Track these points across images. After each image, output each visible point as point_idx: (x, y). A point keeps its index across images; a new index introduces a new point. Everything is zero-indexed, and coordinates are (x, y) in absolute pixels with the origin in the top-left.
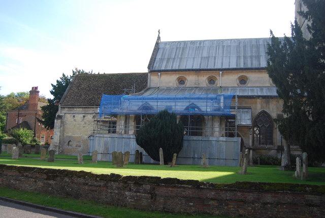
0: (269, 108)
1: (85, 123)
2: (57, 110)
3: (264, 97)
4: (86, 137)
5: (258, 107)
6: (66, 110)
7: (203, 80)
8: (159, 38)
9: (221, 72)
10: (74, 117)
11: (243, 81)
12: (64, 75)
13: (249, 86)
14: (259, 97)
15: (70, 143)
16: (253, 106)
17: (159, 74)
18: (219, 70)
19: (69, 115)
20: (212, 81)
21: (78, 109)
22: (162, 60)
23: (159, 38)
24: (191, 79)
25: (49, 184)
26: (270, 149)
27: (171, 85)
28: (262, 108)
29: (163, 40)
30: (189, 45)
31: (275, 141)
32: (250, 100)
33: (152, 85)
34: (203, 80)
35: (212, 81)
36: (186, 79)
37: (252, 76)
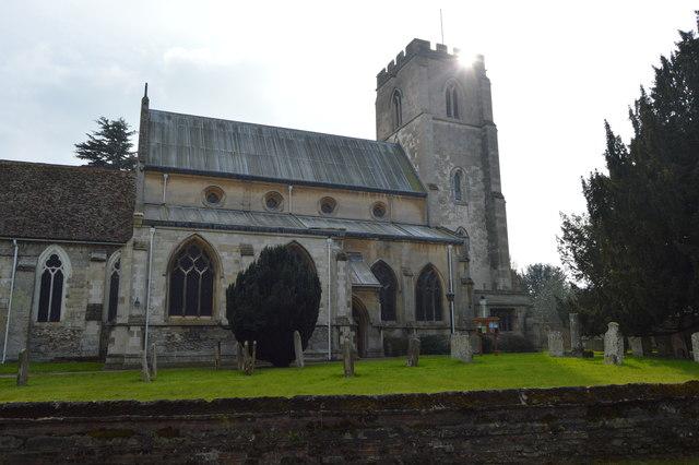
0: (389, 257)
3: (382, 238)
5: (373, 252)
7: (258, 196)
8: (145, 101)
11: (328, 206)
13: (338, 215)
14: (374, 236)
17: (166, 175)
20: (273, 201)
22: (165, 147)
23: (145, 101)
24: (233, 194)
25: (612, 429)
26: (392, 328)
27: (191, 201)
29: (151, 106)
30: (215, 127)
31: (399, 313)
33: (148, 199)
34: (258, 196)
35: (273, 201)
36: (222, 192)
37: (343, 200)
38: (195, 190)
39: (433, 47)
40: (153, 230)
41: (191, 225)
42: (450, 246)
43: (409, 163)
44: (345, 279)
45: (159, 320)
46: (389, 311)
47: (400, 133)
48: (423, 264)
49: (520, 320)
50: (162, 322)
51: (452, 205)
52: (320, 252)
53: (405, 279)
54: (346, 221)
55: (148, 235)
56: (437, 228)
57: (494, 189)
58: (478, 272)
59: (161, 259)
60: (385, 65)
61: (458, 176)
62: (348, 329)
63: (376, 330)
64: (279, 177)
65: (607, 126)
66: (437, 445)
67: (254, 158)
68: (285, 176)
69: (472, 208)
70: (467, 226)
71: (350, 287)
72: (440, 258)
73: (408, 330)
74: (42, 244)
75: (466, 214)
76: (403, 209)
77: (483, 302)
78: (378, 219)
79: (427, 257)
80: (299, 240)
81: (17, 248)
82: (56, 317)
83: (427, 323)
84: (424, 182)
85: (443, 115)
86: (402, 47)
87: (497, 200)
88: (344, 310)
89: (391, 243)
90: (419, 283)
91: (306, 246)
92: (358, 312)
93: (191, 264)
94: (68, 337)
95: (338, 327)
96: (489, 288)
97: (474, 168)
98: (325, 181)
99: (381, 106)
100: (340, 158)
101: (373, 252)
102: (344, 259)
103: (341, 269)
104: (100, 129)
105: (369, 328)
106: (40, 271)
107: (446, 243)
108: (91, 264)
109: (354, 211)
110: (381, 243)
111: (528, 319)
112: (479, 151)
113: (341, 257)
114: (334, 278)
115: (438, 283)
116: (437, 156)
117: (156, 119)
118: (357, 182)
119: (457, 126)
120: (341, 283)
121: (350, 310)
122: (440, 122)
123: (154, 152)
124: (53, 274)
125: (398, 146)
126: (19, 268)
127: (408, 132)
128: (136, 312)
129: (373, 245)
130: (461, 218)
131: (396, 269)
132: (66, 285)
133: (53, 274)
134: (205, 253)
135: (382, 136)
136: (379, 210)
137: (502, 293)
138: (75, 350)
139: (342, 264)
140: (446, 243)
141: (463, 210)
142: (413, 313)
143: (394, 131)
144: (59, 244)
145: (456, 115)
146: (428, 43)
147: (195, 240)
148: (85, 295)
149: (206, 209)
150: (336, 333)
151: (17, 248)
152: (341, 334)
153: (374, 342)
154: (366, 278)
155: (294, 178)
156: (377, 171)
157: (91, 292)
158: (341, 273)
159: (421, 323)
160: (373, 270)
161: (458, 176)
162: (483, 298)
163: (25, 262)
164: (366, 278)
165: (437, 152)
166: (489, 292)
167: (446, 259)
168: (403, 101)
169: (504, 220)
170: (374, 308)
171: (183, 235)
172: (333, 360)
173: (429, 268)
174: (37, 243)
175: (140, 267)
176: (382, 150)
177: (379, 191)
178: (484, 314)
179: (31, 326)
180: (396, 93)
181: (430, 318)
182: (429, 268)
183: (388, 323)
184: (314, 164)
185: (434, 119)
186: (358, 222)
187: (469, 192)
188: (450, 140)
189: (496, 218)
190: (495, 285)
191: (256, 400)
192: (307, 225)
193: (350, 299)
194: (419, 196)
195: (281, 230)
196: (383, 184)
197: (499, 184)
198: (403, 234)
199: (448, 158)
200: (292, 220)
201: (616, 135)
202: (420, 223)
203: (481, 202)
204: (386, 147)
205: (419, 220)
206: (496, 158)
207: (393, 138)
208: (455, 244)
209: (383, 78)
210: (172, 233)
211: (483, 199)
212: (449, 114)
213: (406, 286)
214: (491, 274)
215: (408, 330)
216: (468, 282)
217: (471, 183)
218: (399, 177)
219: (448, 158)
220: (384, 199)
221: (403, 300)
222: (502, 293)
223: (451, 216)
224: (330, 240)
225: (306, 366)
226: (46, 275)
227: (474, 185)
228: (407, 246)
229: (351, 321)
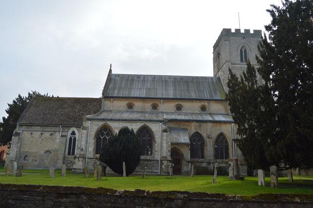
0: (201, 130)
1: (43, 140)
2: (15, 127)
3: (197, 121)
4: (43, 152)
5: (193, 128)
6: (24, 128)
7: (148, 106)
8: (110, 71)
10: (32, 134)
11: (179, 108)
12: (19, 96)
13: (183, 112)
14: (193, 121)
15: (26, 158)
16: (189, 128)
18: (161, 99)
19: (26, 133)
20: (155, 107)
21: (36, 127)
22: (114, 88)
23: (110, 71)
24: (138, 105)
26: (202, 162)
27: (121, 109)
29: (113, 72)
30: (136, 78)
31: (205, 155)
32: (186, 123)
33: (106, 109)
34: (148, 106)
35: (155, 107)
36: (134, 105)
37: (186, 105)
38: (123, 104)
40: (90, 122)
41: (103, 120)
42: (233, 124)
44: (166, 140)
45: (91, 156)
48: (218, 133)
50: (92, 157)
53: (208, 140)
54: (186, 114)
55: (87, 124)
59: (92, 133)
64: (158, 97)
66: (10, 201)
67: (148, 90)
68: (160, 96)
71: (170, 144)
73: (209, 163)
74: (69, 127)
78: (203, 112)
80: (147, 124)
85: (239, 62)
89: (202, 124)
91: (150, 127)
98: (178, 97)
100: (188, 86)
103: (165, 136)
105: (184, 162)
106: (69, 137)
110: (196, 124)
113: (165, 131)
117: (114, 77)
118: (193, 96)
120: (165, 142)
121: (169, 154)
122: (236, 65)
125: (219, 79)
126: (62, 136)
127: (222, 71)
128: (82, 153)
129: (193, 124)
131: (204, 135)
136: (203, 108)
139: (165, 134)
146: (230, 30)
147: (105, 125)
149: (127, 111)
152: (163, 164)
154: (184, 139)
156: (205, 91)
158: (165, 138)
163: (64, 134)
167: (230, 130)
171: (101, 123)
172: (160, 175)
173: (222, 134)
175: (84, 136)
177: (203, 100)
179: (64, 158)
181: (222, 158)
182: (222, 134)
185: (232, 64)
196: (206, 96)
198: (211, 119)
201: (234, 73)
202: (225, 113)
205: (224, 112)
212: (242, 61)
213: (208, 143)
215: (209, 163)
218: (215, 92)
220: (206, 103)
226: (71, 138)
228: (210, 125)
229: (169, 158)
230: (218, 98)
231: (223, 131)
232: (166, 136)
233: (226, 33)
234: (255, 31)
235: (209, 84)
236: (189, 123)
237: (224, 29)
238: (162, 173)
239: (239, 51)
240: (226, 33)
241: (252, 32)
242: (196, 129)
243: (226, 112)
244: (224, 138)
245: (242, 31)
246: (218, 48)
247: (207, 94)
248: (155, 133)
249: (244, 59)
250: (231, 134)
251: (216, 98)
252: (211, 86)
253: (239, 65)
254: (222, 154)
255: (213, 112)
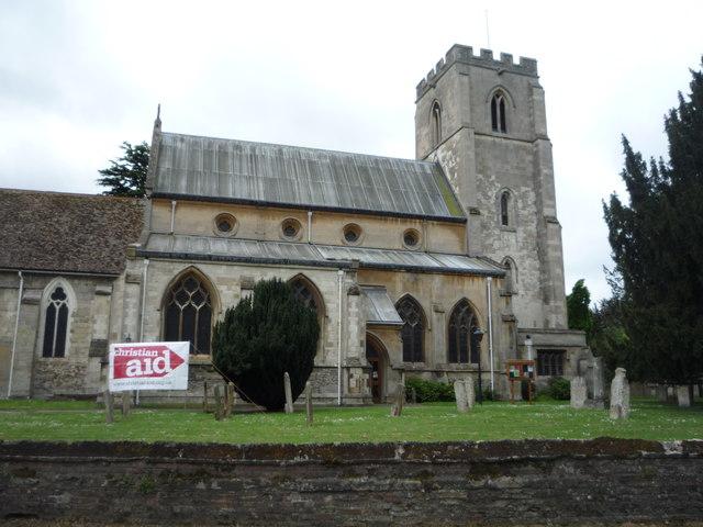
0: (418, 291)
5: (399, 286)
7: (274, 224)
8: (158, 124)
9: (310, 213)
13: (364, 244)
17: (174, 203)
22: (176, 172)
23: (158, 124)
24: (246, 221)
25: (494, 489)
26: (420, 371)
27: (200, 229)
28: (404, 291)
29: (164, 129)
30: (230, 149)
31: (428, 354)
33: (157, 228)
34: (274, 224)
36: (234, 220)
37: (368, 227)
38: (206, 217)
39: (477, 53)
40: (146, 262)
41: (186, 257)
42: (489, 279)
43: (449, 186)
46: (414, 350)
47: (439, 151)
48: (458, 298)
49: (573, 362)
51: (497, 232)
52: (330, 286)
54: (372, 250)
55: (141, 268)
56: (477, 257)
57: (547, 212)
58: (526, 309)
59: (156, 294)
60: (424, 76)
61: (505, 198)
62: (359, 371)
63: (397, 373)
64: (298, 202)
65: (626, 142)
66: (295, 499)
67: (270, 182)
68: (305, 202)
69: (521, 234)
70: (514, 254)
71: (363, 324)
72: (476, 291)
73: (438, 373)
74: (47, 275)
75: (514, 241)
76: (438, 236)
77: (528, 343)
79: (462, 291)
80: (306, 273)
81: (22, 281)
82: (60, 352)
83: (461, 366)
84: (464, 206)
85: (489, 130)
86: (440, 54)
87: (551, 226)
88: (356, 348)
89: (421, 276)
90: (452, 320)
91: (314, 279)
92: (374, 351)
93: (187, 298)
94: (73, 374)
95: (348, 368)
96: (540, 325)
97: (523, 189)
98: (350, 206)
99: (420, 121)
101: (399, 286)
102: (357, 293)
103: (354, 304)
104: (123, 154)
106: (45, 305)
107: (484, 275)
108: (96, 297)
109: (379, 246)
110: (407, 276)
111: (582, 362)
112: (530, 169)
113: (354, 292)
114: (345, 314)
115: (475, 321)
116: (480, 176)
117: (168, 142)
118: (386, 206)
119: (504, 141)
121: (363, 350)
122: (483, 138)
123: (164, 178)
124: (58, 308)
125: (437, 166)
126: (25, 302)
127: (448, 149)
129: (399, 278)
130: (510, 245)
131: (426, 304)
132: (70, 320)
133: (58, 308)
134: (202, 286)
135: (422, 154)
136: (410, 238)
137: (552, 332)
138: (79, 387)
139: (354, 299)
140: (484, 275)
141: (511, 238)
142: (444, 353)
143: (435, 149)
144: (64, 276)
145: (504, 129)
146: (469, 49)
148: (90, 331)
149: (217, 237)
150: (346, 376)
151: (22, 281)
152: (351, 376)
153: (393, 385)
154: (387, 313)
155: (314, 204)
157: (96, 327)
159: (454, 366)
160: (397, 307)
161: (505, 198)
162: (528, 337)
163: (30, 295)
164: (387, 313)
165: (480, 172)
166: (535, 331)
167: (484, 294)
168: (443, 114)
169: (559, 248)
170: (394, 348)
171: (179, 268)
173: (464, 303)
174: (44, 275)
175: (133, 301)
176: (418, 170)
178: (530, 356)
179: (35, 363)
180: (436, 106)
181: (464, 360)
182: (464, 303)
183: (415, 365)
184: (339, 188)
186: (386, 251)
187: (518, 216)
188: (496, 157)
189: (548, 246)
190: (547, 322)
191: (116, 444)
192: (325, 255)
193: (364, 338)
194: (456, 223)
195: (286, 262)
197: (554, 207)
198: (434, 264)
199: (493, 178)
200: (309, 250)
201: (635, 151)
202: (460, 252)
203: (532, 228)
204: (422, 167)
206: (551, 177)
207: (432, 156)
208: (495, 276)
209: (423, 89)
210: (167, 265)
211: (534, 225)
212: (494, 127)
213: (435, 321)
214: (543, 309)
216: (510, 321)
217: (520, 205)
218: (435, 200)
219: (493, 178)
220: (416, 226)
221: (433, 338)
222: (552, 332)
223: (496, 244)
224: (341, 272)
225: (295, 411)
226: (51, 309)
227: (524, 208)
228: (438, 279)
229: (364, 363)
230: (443, 214)
231: (466, 296)
232: (357, 305)
233: (460, 56)
234: (524, 60)
235: (417, 180)
236: (390, 274)
237: (456, 46)
238: (348, 402)
239: (489, 104)
240: (460, 56)
241: (516, 61)
242: (405, 289)
243: (462, 249)
244: (470, 311)
245: (497, 57)
246: (432, 91)
247: (417, 202)
248: (326, 297)
249: (499, 125)
250: (484, 302)
251: (437, 214)
252: (423, 183)
253: (489, 138)
254: (464, 351)
255: (433, 248)
